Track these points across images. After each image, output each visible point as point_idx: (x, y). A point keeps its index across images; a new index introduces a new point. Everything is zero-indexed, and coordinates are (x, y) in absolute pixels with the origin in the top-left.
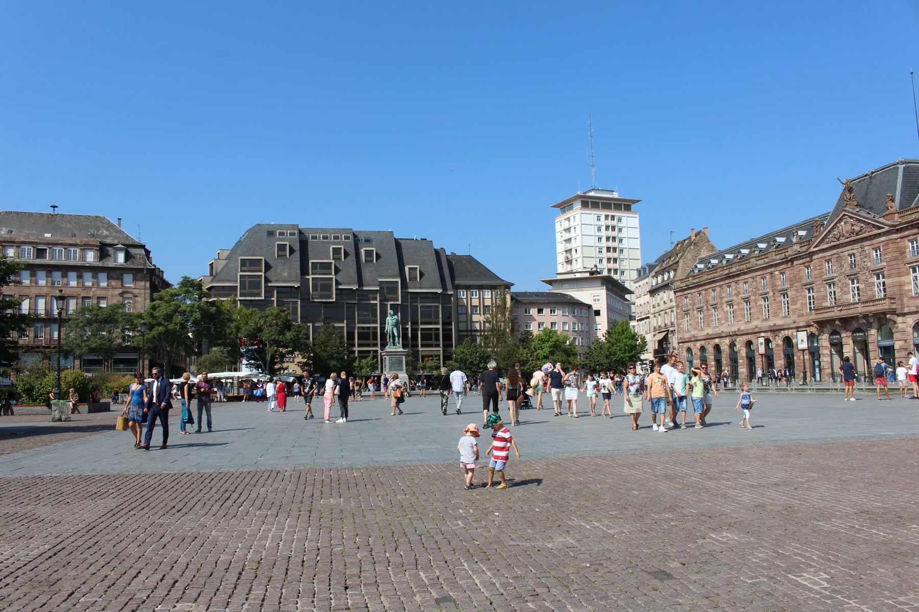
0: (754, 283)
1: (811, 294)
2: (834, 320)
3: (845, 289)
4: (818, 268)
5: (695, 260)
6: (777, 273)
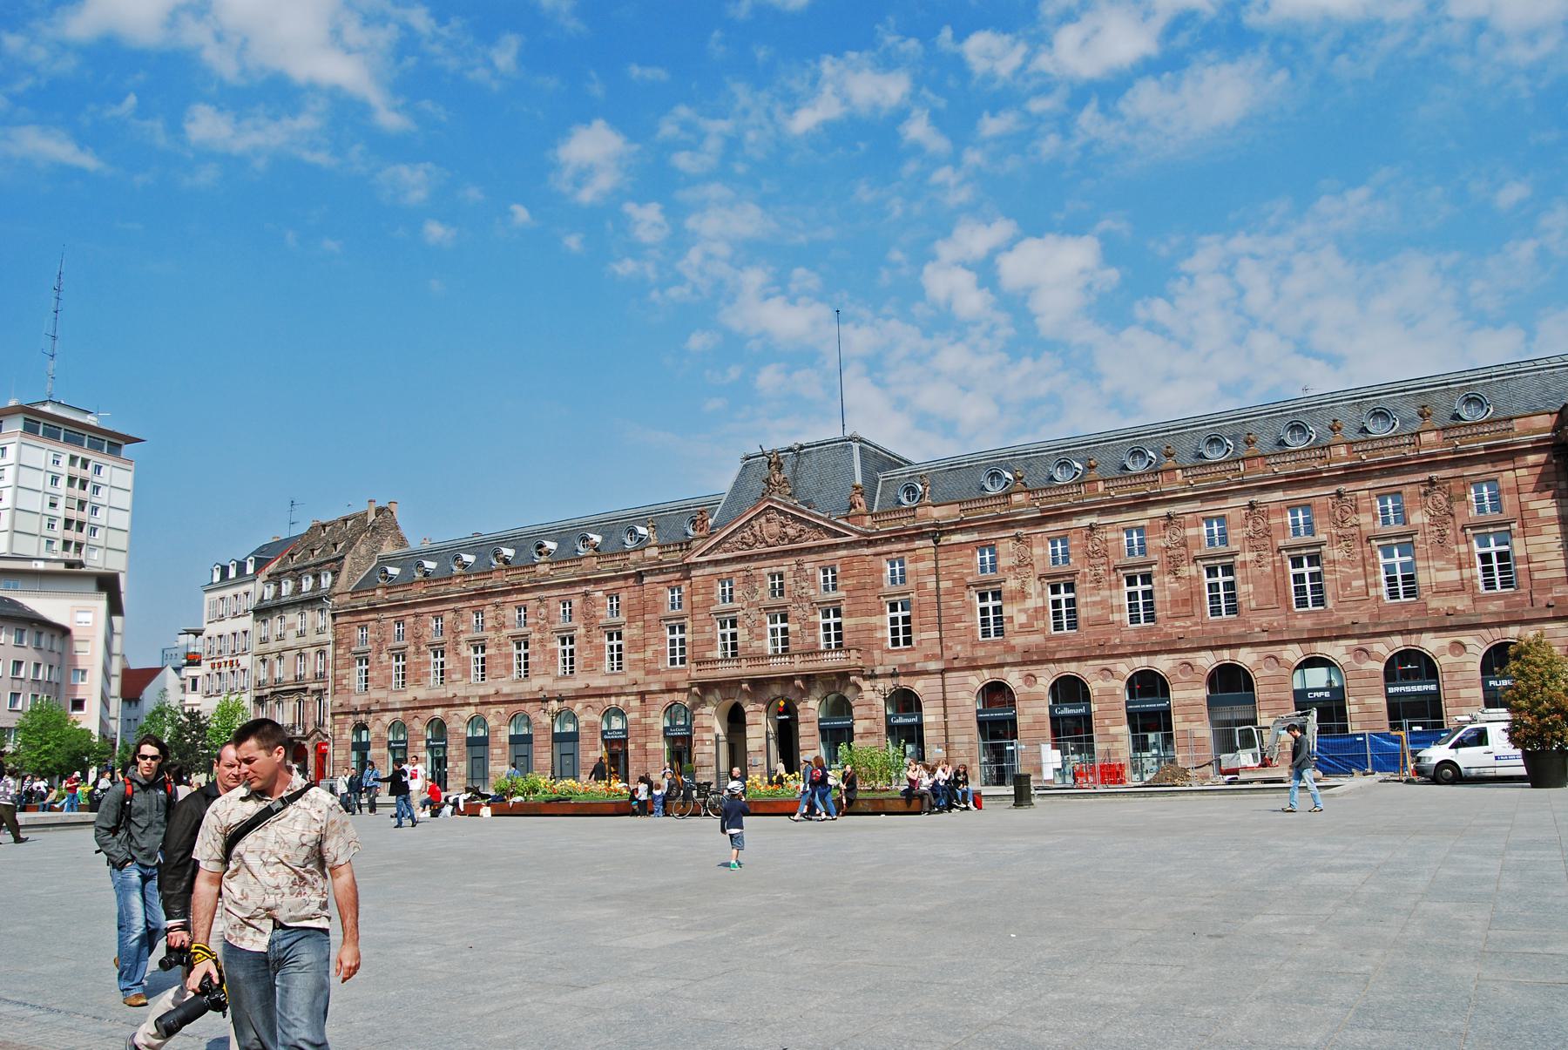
0: (543, 610)
1: (678, 636)
2: (740, 682)
3: (757, 631)
4: (703, 591)
5: (371, 559)
6: (600, 594)
